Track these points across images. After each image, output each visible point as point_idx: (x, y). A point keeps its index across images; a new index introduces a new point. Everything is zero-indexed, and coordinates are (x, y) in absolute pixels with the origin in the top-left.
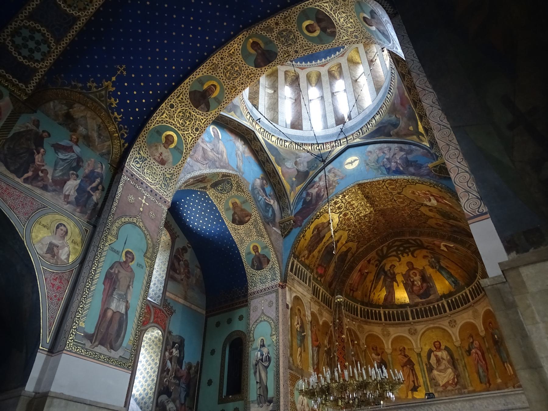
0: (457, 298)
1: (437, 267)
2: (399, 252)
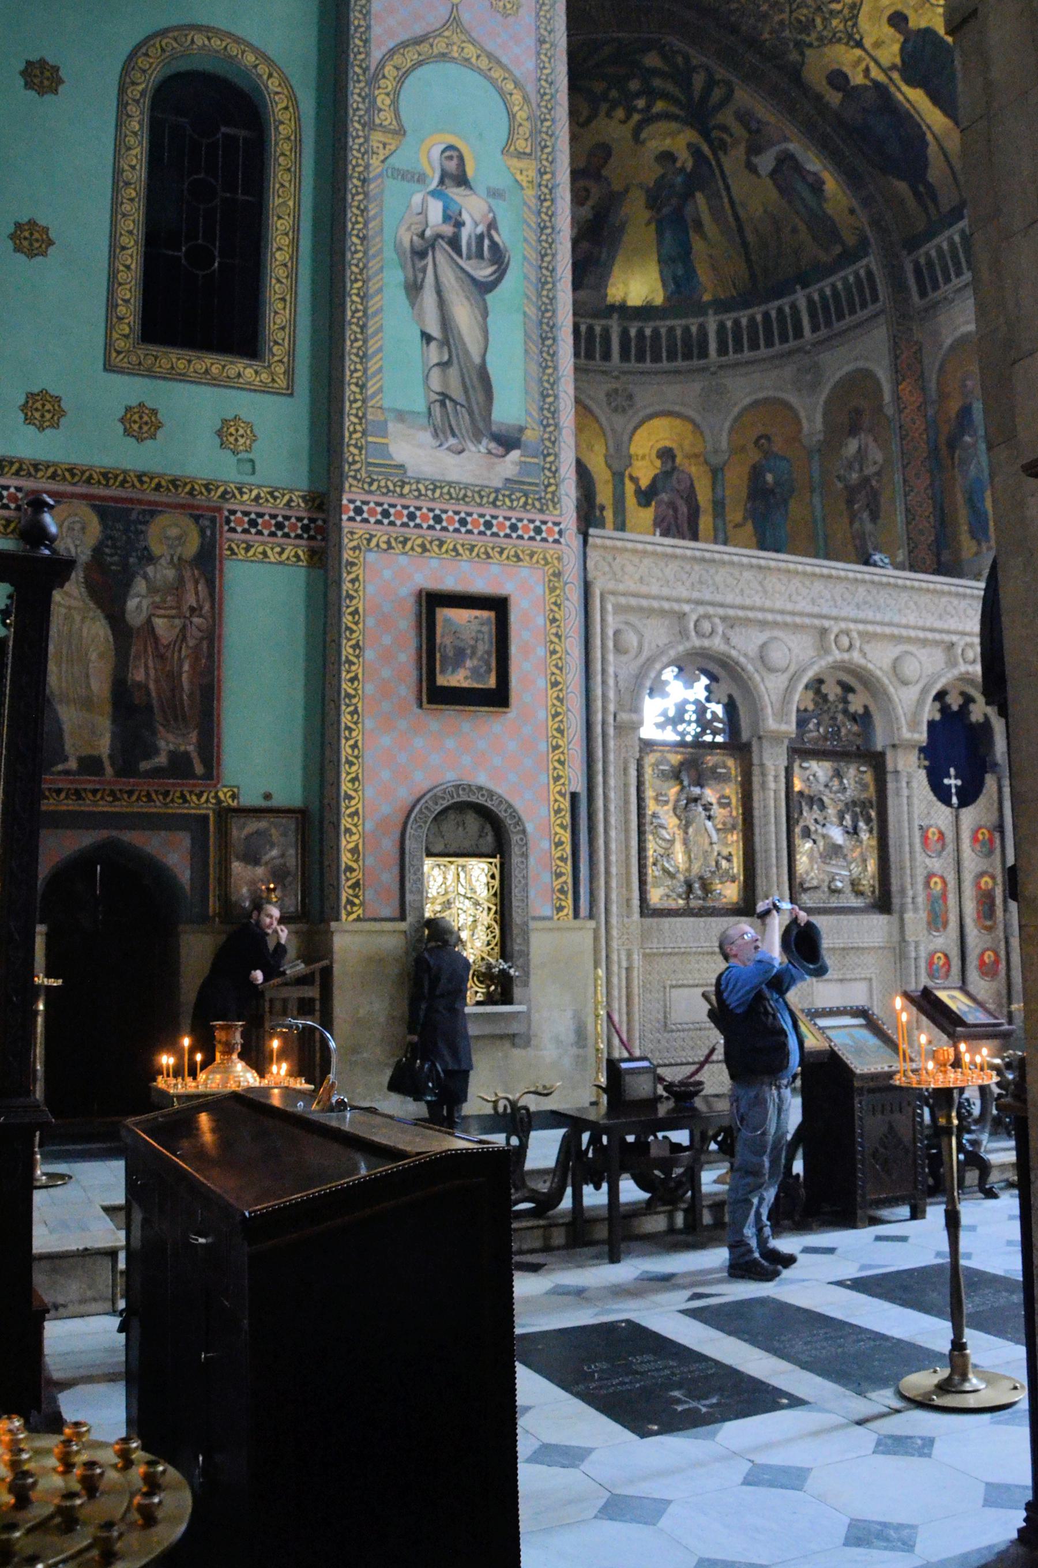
0: (663, 331)
1: (666, 211)
2: (614, 94)
